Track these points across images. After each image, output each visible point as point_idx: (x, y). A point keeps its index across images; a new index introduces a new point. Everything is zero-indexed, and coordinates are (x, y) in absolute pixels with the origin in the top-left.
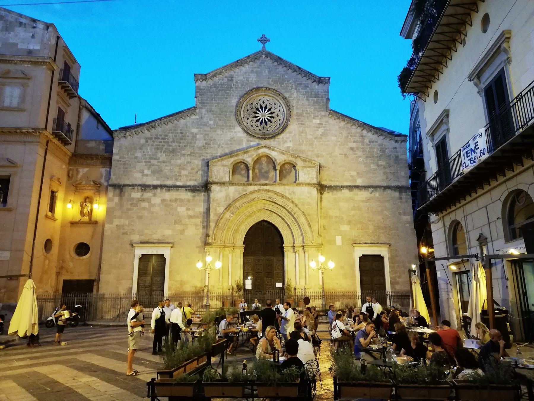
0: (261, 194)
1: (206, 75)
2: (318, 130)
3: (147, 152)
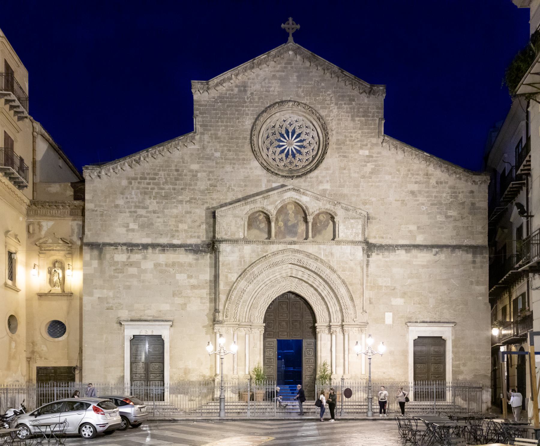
0: (286, 256)
2: (366, 166)
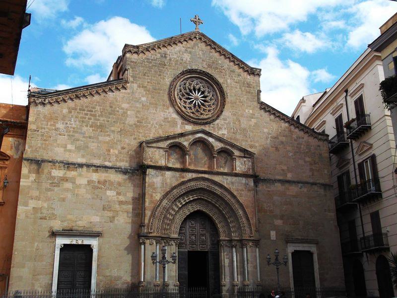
1: (138, 47)
3: (71, 124)
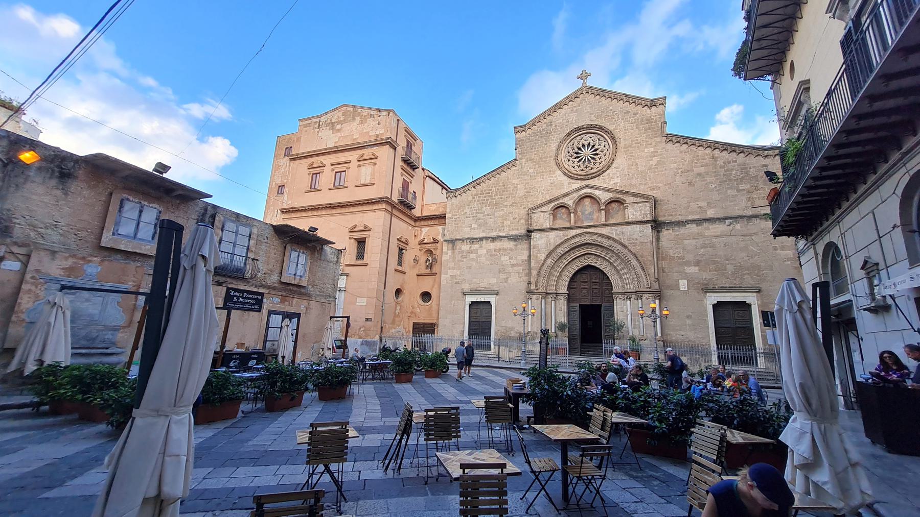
1: (525, 126)
